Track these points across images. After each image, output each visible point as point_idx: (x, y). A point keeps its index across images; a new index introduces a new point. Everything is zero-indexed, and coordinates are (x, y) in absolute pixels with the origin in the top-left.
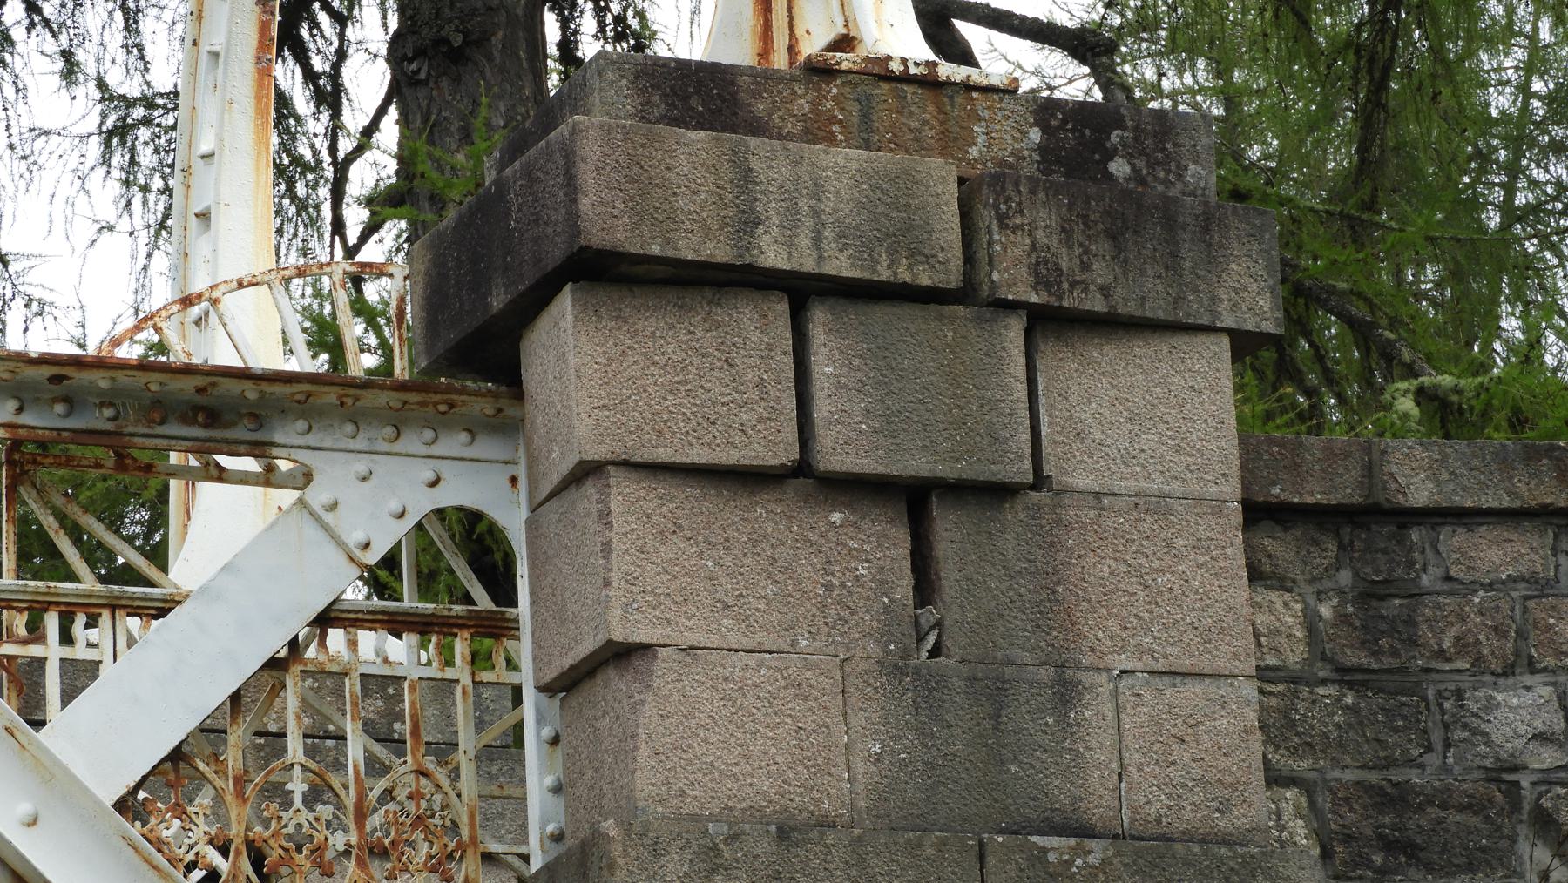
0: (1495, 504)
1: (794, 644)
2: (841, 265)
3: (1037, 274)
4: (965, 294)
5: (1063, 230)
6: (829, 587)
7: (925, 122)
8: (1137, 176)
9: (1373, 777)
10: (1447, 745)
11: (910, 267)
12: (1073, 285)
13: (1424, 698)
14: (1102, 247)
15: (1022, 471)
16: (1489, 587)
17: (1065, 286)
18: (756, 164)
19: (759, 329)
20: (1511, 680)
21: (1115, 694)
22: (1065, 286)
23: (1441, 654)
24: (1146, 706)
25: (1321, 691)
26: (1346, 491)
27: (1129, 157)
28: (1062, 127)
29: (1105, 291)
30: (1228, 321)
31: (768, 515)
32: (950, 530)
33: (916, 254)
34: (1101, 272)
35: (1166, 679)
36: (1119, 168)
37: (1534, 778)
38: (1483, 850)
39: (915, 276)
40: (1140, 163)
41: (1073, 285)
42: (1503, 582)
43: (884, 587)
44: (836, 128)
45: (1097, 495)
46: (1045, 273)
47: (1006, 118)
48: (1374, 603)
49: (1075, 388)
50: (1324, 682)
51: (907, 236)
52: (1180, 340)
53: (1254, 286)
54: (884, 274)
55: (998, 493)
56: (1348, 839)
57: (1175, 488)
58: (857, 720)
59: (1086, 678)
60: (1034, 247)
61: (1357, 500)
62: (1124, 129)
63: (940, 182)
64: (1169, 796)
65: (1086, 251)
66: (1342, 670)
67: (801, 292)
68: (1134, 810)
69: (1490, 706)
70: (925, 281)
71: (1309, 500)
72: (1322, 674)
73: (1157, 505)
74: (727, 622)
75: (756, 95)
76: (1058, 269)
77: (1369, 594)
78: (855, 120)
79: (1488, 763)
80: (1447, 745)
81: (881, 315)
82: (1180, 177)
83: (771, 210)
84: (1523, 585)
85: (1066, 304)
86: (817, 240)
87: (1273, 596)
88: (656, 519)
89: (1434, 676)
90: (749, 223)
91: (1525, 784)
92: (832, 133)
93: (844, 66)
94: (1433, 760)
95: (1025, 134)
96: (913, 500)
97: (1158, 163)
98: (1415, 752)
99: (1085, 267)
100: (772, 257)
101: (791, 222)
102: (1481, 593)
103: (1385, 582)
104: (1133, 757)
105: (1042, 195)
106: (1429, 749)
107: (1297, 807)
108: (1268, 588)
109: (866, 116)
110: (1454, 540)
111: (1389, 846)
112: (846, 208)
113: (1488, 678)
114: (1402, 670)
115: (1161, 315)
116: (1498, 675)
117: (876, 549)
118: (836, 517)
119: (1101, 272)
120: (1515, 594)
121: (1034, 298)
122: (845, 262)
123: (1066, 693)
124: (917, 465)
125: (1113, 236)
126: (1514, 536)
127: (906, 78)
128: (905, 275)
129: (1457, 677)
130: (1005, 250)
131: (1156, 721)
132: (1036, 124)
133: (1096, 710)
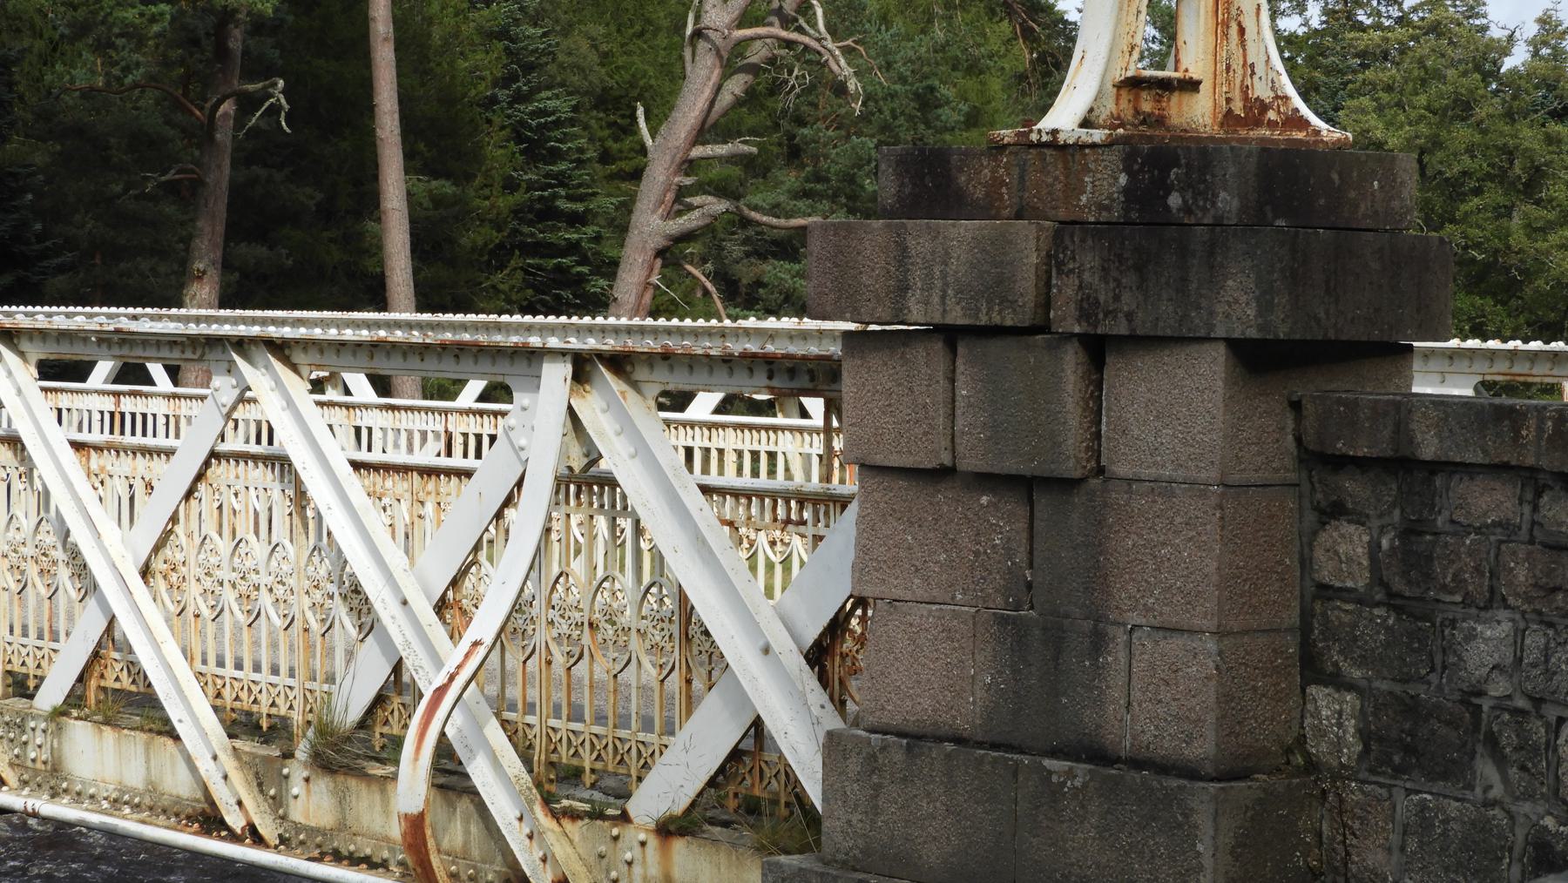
0: (1473, 460)
1: (953, 598)
2: (956, 317)
3: (1081, 309)
4: (1042, 328)
5: (1104, 269)
6: (977, 554)
7: (1056, 178)
8: (1187, 209)
9: (1398, 689)
10: (1444, 668)
11: (1000, 312)
12: (1106, 316)
13: (1433, 625)
14: (1130, 279)
15: (1070, 468)
16: (1478, 531)
17: (1101, 316)
18: (911, 242)
20: (1489, 614)
21: (1130, 643)
22: (1101, 316)
23: (1444, 588)
25: (1376, 611)
26: (1384, 449)
27: (1182, 191)
28: (1141, 170)
29: (1129, 316)
30: (1220, 332)
31: (944, 497)
33: (1006, 302)
34: (1128, 301)
35: (1161, 633)
36: (1174, 200)
37: (1492, 703)
38: (1453, 761)
39: (1003, 318)
40: (1189, 195)
41: (1106, 316)
42: (1487, 526)
43: (1009, 553)
44: (1004, 190)
45: (1130, 481)
46: (1088, 307)
47: (1106, 167)
48: (1413, 538)
49: (1125, 392)
50: (1378, 604)
51: (998, 288)
52: (1193, 349)
53: (1244, 299)
54: (983, 320)
55: (1068, 485)
56: (1381, 740)
57: (1180, 474)
58: (980, 658)
59: (1111, 630)
60: (1080, 287)
61: (1389, 453)
62: (1179, 166)
64: (1157, 727)
65: (1119, 284)
66: (1391, 595)
67: (950, 335)
68: (1134, 737)
69: (1471, 636)
70: (1009, 323)
71: (1360, 454)
72: (1378, 597)
73: (1162, 487)
74: (917, 581)
75: (960, 170)
76: (1097, 301)
77: (1410, 532)
78: (1015, 182)
79: (1465, 686)
80: (1444, 668)
81: (995, 346)
82: (1214, 204)
83: (917, 277)
84: (1499, 530)
85: (1099, 331)
86: (943, 297)
87: (1352, 528)
88: (882, 505)
89: (1441, 606)
91: (1485, 708)
92: (1002, 194)
93: (1006, 140)
94: (1433, 678)
95: (1116, 179)
96: (1024, 486)
97: (1200, 194)
98: (1423, 672)
99: (1117, 298)
101: (928, 288)
102: (1472, 536)
103: (1418, 521)
104: (1136, 694)
105: (1090, 242)
106: (1433, 670)
107: (1353, 708)
108: (1349, 522)
109: (1022, 178)
110: (1461, 487)
111: (1409, 750)
112: (963, 269)
113: (1473, 611)
114: (1421, 599)
115: (1169, 332)
116: (1481, 609)
117: (1002, 523)
118: (984, 500)
119: (1128, 301)
120: (1492, 538)
121: (1077, 329)
122: (960, 313)
123: (1098, 642)
125: (1139, 269)
126: (1498, 485)
127: (1040, 145)
128: (997, 319)
129: (1453, 608)
130: (1060, 291)
131: (1152, 666)
132: (1124, 170)
133: (1115, 657)
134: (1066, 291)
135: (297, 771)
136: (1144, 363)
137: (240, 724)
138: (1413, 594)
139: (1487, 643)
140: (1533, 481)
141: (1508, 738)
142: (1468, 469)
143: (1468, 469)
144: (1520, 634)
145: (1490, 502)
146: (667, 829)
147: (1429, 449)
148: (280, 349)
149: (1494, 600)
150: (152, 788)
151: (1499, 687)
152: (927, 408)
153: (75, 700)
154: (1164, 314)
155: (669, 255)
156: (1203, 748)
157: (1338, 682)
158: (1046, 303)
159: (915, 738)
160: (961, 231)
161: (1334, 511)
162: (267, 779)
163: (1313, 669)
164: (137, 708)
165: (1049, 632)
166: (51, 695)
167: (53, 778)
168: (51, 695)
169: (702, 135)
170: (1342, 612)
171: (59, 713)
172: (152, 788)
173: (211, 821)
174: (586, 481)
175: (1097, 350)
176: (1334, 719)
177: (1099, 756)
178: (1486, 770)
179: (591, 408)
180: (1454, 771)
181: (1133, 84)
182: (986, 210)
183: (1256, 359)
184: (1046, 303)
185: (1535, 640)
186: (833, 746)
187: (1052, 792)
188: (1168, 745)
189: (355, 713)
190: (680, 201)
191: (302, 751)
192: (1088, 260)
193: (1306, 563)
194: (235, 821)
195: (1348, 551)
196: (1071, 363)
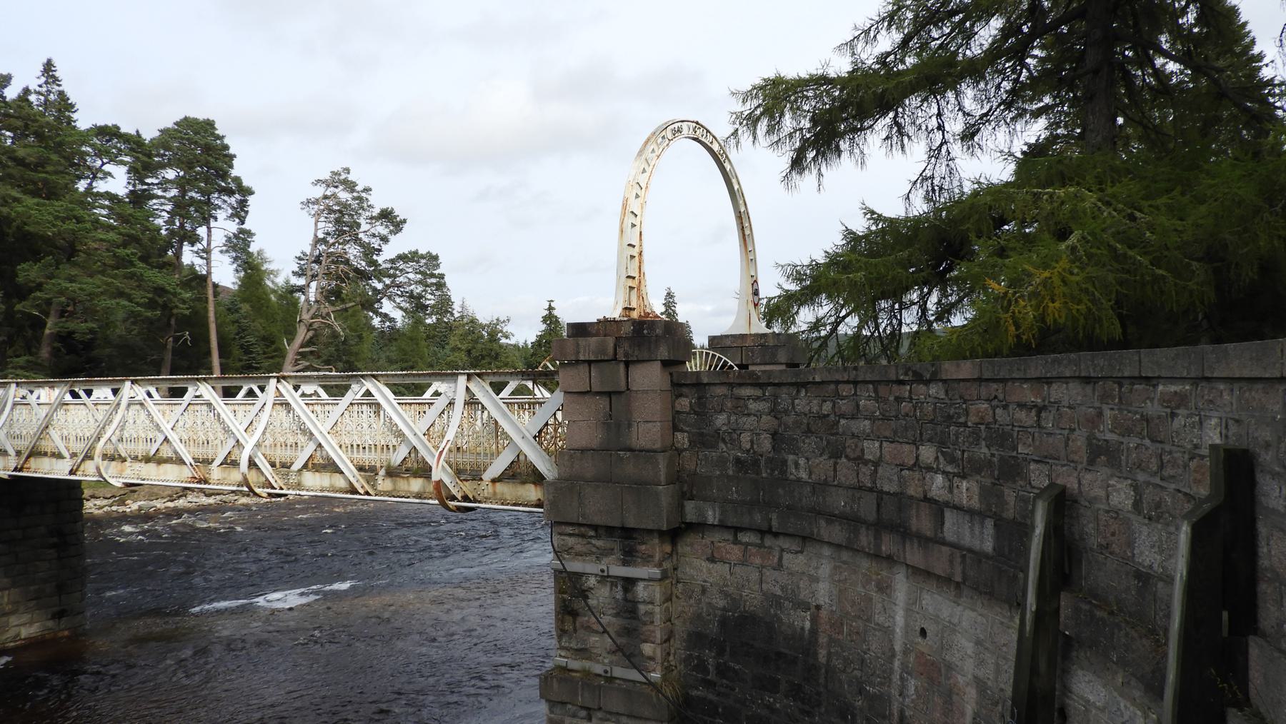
2: (592, 358)
15: (623, 388)
19: (583, 369)
24: (642, 427)
32: (614, 398)
46: (626, 355)
55: (620, 393)
63: (610, 342)
67: (590, 362)
73: (646, 392)
77: (699, 398)
90: (578, 353)
96: (609, 394)
100: (582, 358)
110: (712, 388)
117: (603, 403)
123: (630, 426)
124: (606, 389)
133: (634, 429)
134: (620, 352)
135: (380, 479)
136: (640, 366)
138: (701, 411)
139: (721, 420)
140: (731, 385)
141: (727, 439)
142: (714, 384)
143: (714, 384)
144: (729, 418)
146: (494, 481)
147: (705, 380)
148: (374, 376)
149: (722, 411)
150: (332, 486)
151: (724, 428)
153: (305, 466)
154: (646, 356)
156: (658, 446)
157: (682, 431)
158: (615, 354)
159: (583, 451)
160: (594, 339)
161: (681, 395)
162: (371, 481)
163: (675, 428)
164: (330, 466)
166: (296, 467)
167: (299, 486)
168: (296, 467)
169: (302, 346)
170: (683, 417)
171: (300, 470)
172: (332, 486)
173: (354, 491)
174: (472, 402)
175: (627, 364)
176: (682, 439)
177: (631, 450)
178: (722, 445)
179: (472, 386)
180: (714, 446)
181: (626, 308)
182: (597, 335)
183: (666, 364)
184: (615, 354)
185: (733, 418)
187: (622, 459)
188: (649, 446)
189: (398, 462)
191: (382, 472)
192: (626, 345)
193: (673, 407)
194: (361, 491)
195: (684, 403)
196: (622, 366)
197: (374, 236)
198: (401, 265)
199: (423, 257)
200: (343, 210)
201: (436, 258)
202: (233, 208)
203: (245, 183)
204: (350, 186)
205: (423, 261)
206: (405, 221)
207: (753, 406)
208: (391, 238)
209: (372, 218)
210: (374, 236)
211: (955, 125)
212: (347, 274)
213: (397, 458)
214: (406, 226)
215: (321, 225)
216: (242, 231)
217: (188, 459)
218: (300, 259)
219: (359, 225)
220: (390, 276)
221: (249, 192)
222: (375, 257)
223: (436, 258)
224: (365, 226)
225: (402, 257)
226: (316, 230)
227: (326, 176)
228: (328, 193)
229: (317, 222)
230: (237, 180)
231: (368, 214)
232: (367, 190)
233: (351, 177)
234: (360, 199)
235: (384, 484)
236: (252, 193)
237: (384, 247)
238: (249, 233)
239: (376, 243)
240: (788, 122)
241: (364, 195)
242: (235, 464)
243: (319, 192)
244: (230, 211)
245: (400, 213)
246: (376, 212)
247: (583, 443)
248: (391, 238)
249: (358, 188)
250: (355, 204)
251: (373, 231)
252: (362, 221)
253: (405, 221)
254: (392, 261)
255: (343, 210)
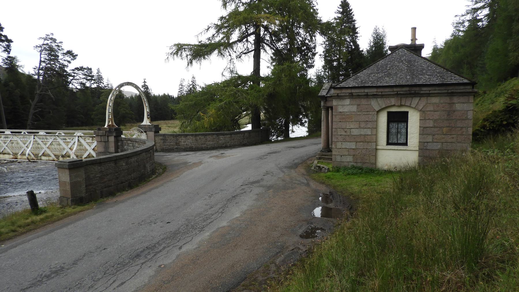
117: (104, 143)
137: (55, 156)
139: (125, 147)
145: (125, 142)
152: (99, 139)
155: (34, 114)
165: (106, 148)
166: (40, 155)
168: (40, 155)
169: (38, 102)
186: (96, 153)
190: (35, 109)
197: (65, 60)
198: (76, 71)
199: (85, 69)
200: (51, 50)
201: (91, 69)
202: (4, 47)
203: (9, 38)
204: (54, 40)
205: (86, 70)
206: (77, 55)
207: (130, 145)
208: (72, 61)
209: (64, 53)
210: (65, 60)
211: (234, 55)
212: (55, 75)
213: (64, 153)
214: (77, 57)
215: (42, 56)
216: (9, 57)
217: (11, 153)
218: (35, 69)
219: (58, 56)
220: (72, 76)
221: (10, 41)
222: (66, 69)
223: (91, 69)
224: (61, 57)
225: (77, 69)
226: (41, 58)
227: (44, 36)
228: (45, 43)
229: (41, 54)
230: (5, 36)
231: (62, 52)
232: (61, 42)
233: (54, 37)
234: (58, 46)
235: (61, 159)
236: (12, 42)
237: (69, 65)
238: (13, 58)
239: (66, 63)
240: (184, 54)
241: (60, 44)
242: (25, 155)
243: (41, 42)
244: (3, 49)
245: (75, 52)
246: (65, 51)
247: (100, 151)
248: (72, 61)
249: (57, 42)
250: (56, 48)
251: (64, 59)
252: (59, 55)
253: (77, 55)
254: (73, 70)
255: (51, 50)
